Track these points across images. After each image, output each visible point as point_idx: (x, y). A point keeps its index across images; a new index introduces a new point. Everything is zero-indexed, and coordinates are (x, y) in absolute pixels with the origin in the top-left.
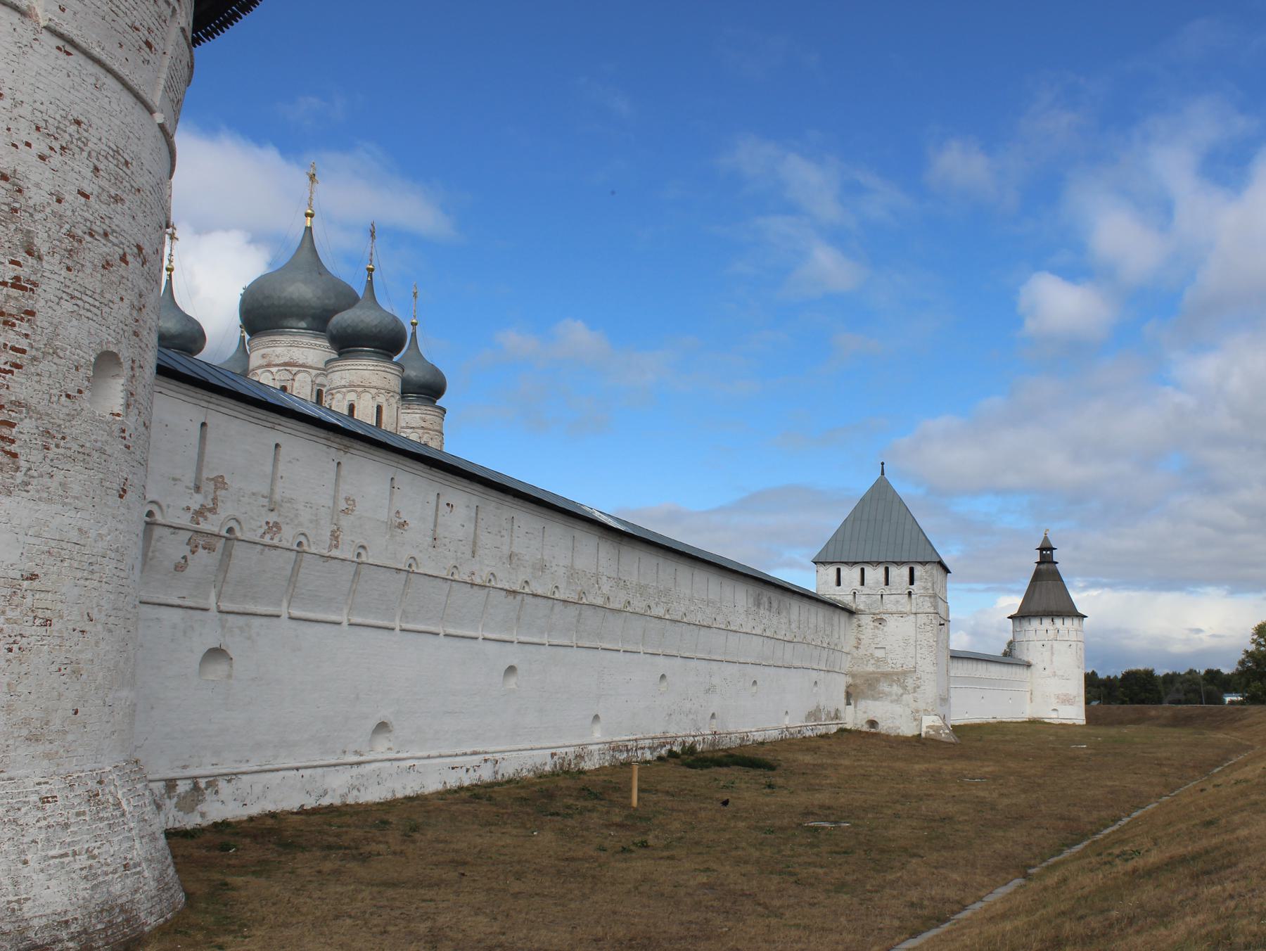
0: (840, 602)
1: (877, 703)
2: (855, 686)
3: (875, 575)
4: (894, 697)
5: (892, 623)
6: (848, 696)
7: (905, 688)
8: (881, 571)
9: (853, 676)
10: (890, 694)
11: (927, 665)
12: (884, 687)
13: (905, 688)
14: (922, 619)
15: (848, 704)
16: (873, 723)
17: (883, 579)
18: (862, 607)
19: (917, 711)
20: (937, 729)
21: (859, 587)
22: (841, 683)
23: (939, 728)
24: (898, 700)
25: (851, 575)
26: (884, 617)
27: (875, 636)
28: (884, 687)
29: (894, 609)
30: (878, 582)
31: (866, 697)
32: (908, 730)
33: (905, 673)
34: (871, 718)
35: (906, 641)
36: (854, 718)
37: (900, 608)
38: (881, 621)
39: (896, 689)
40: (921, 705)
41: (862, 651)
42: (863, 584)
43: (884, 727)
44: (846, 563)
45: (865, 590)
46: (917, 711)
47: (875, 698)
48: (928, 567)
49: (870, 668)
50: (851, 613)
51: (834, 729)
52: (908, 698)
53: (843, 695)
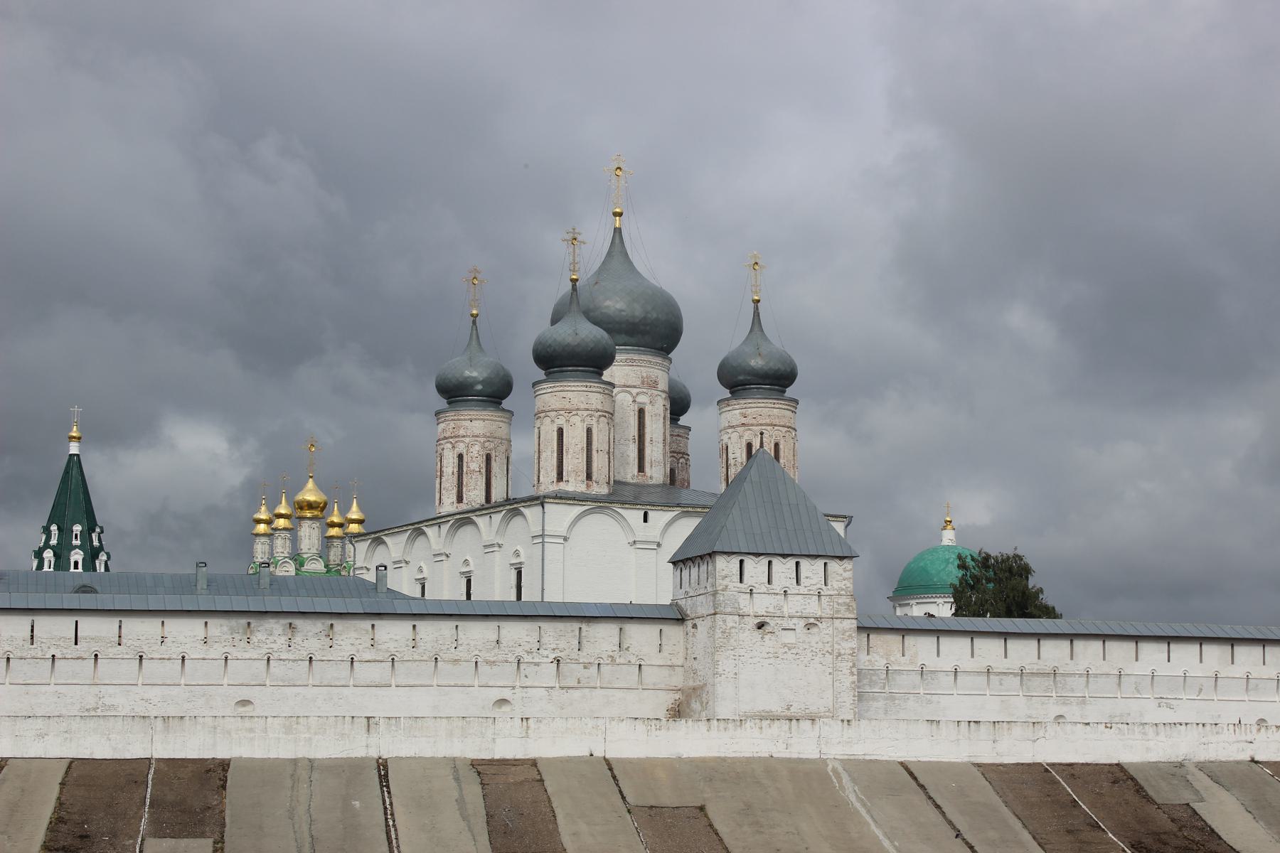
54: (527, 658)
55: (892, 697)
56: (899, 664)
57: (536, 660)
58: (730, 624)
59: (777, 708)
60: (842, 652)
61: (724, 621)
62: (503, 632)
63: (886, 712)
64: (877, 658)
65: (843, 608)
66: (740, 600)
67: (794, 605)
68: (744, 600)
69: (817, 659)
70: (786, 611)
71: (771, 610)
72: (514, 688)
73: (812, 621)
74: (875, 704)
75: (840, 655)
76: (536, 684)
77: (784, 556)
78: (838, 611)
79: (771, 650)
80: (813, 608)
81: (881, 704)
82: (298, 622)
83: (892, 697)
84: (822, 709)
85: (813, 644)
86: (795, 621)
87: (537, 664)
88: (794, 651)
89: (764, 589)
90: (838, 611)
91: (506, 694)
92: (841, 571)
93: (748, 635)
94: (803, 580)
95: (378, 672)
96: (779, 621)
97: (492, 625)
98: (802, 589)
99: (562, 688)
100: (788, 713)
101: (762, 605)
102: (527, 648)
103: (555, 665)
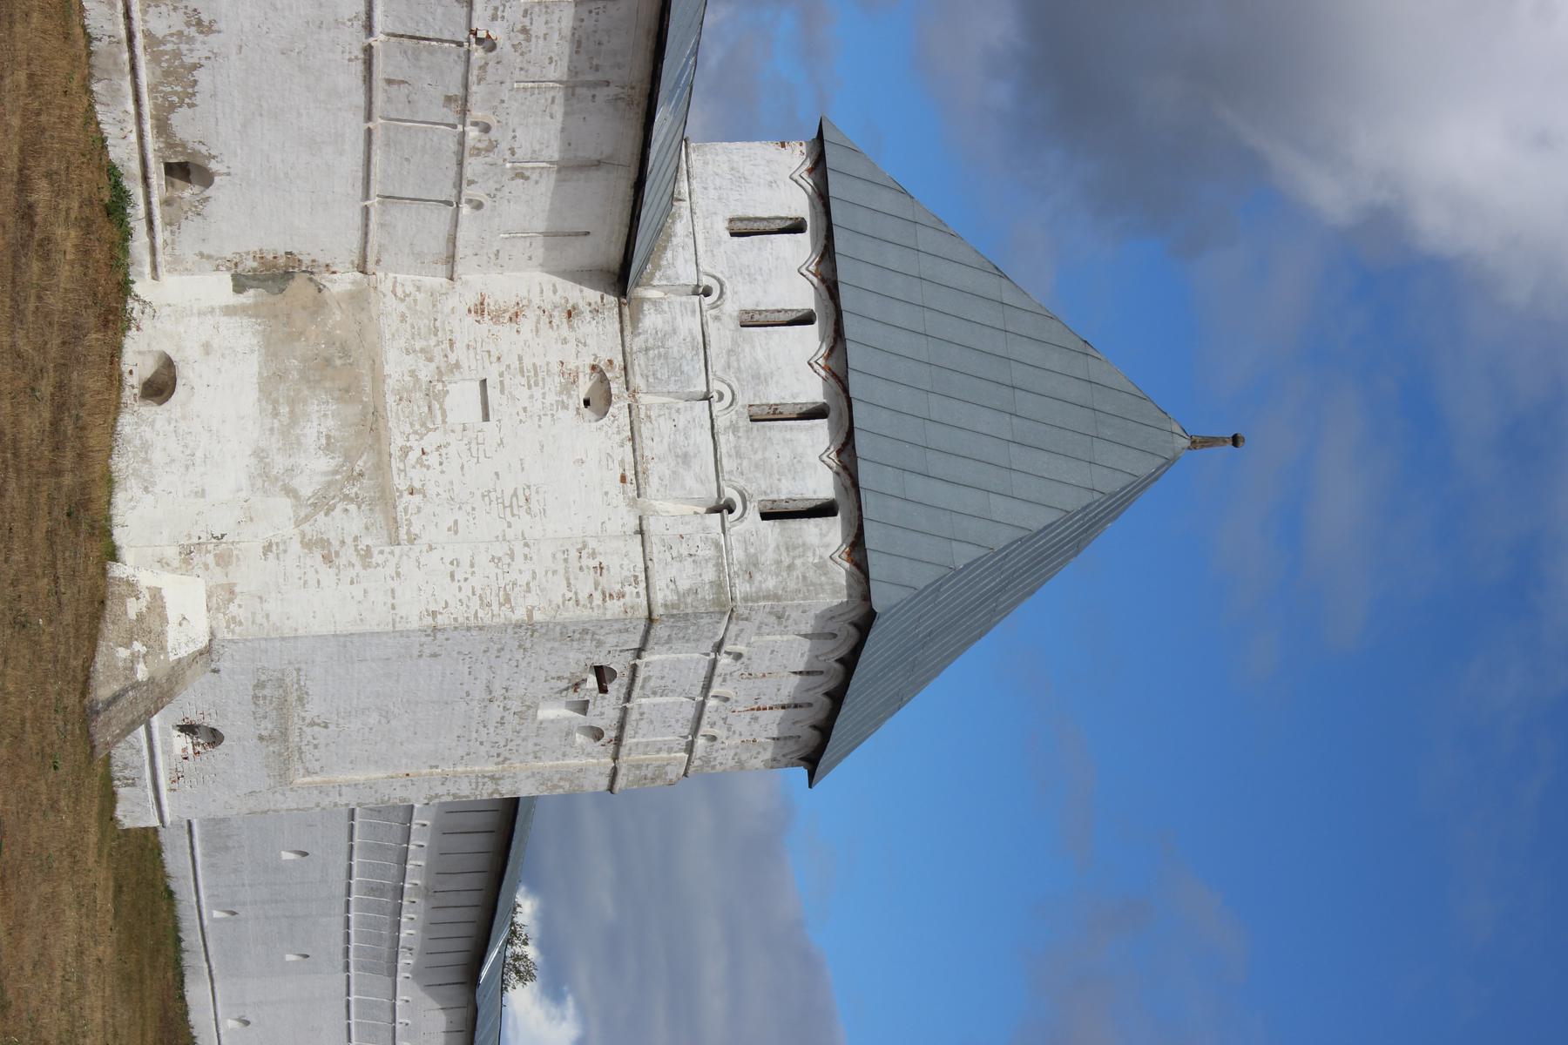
0: (662, 232)
1: (252, 394)
2: (318, 306)
3: (793, 365)
4: (279, 463)
5: (599, 441)
6: (271, 276)
7: (322, 503)
8: (813, 390)
9: (359, 299)
10: (289, 438)
11: (424, 584)
12: (321, 418)
13: (322, 503)
14: (623, 559)
15: (240, 285)
16: (160, 387)
17: (774, 394)
18: (651, 320)
19: (223, 560)
20: (150, 628)
21: (731, 307)
22: (321, 230)
23: (156, 641)
24: (266, 477)
25: (786, 273)
26: (619, 408)
27: (533, 378)
28: (321, 418)
29: (653, 446)
30: (758, 378)
31: (271, 349)
32: (144, 523)
33: (384, 499)
34: (184, 374)
35: (522, 501)
36: (180, 302)
37: (657, 472)
38: (598, 402)
39: (314, 468)
40: (250, 574)
41: (466, 329)
42: (751, 321)
43: (140, 425)
44: (827, 252)
45: (722, 334)
46: (223, 560)
47: (270, 384)
48: (841, 572)
49: (396, 365)
50: (620, 279)
51: (122, 152)
52: (279, 516)
53: (276, 244)
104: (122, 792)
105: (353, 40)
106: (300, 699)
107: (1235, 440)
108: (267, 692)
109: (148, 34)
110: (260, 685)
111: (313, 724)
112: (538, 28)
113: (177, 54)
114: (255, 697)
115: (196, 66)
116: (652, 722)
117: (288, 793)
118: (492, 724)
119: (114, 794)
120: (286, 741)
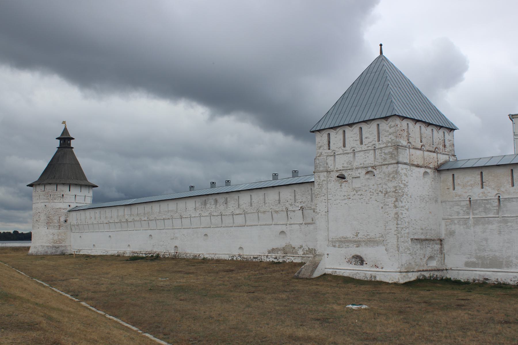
54: (290, 208)
55: (505, 220)
56: (509, 193)
57: (294, 209)
58: (322, 178)
59: (350, 235)
60: (389, 190)
61: (319, 177)
62: (253, 197)
63: (500, 233)
64: (490, 190)
65: (388, 157)
66: (328, 161)
67: (361, 159)
68: (330, 160)
69: (373, 197)
70: (356, 164)
71: (345, 165)
72: (286, 225)
73: (370, 169)
74: (490, 227)
75: (387, 192)
76: (295, 222)
77: (350, 125)
78: (385, 160)
79: (346, 194)
80: (369, 159)
81: (495, 226)
82: (217, 197)
83: (505, 220)
84: (378, 235)
85: (371, 186)
86: (360, 171)
87: (294, 211)
88: (359, 193)
89: (341, 151)
90: (385, 160)
91: (284, 228)
92: (388, 128)
93: (333, 185)
94: (364, 140)
95: (239, 220)
96: (350, 172)
97: (277, 190)
98: (364, 147)
99: (305, 224)
100: (356, 239)
101: (340, 163)
102: (290, 203)
103: (301, 211)
104: (378, 279)
105: (303, 227)
106: (345, 238)
107: (381, 45)
108: (337, 245)
109: (303, 254)
110: (334, 246)
111: (357, 236)
112: (300, 200)
113: (306, 251)
114: (339, 247)
115: (309, 248)
116: (365, 161)
117: (388, 241)
118: (362, 197)
119: (378, 281)
120: (360, 241)
